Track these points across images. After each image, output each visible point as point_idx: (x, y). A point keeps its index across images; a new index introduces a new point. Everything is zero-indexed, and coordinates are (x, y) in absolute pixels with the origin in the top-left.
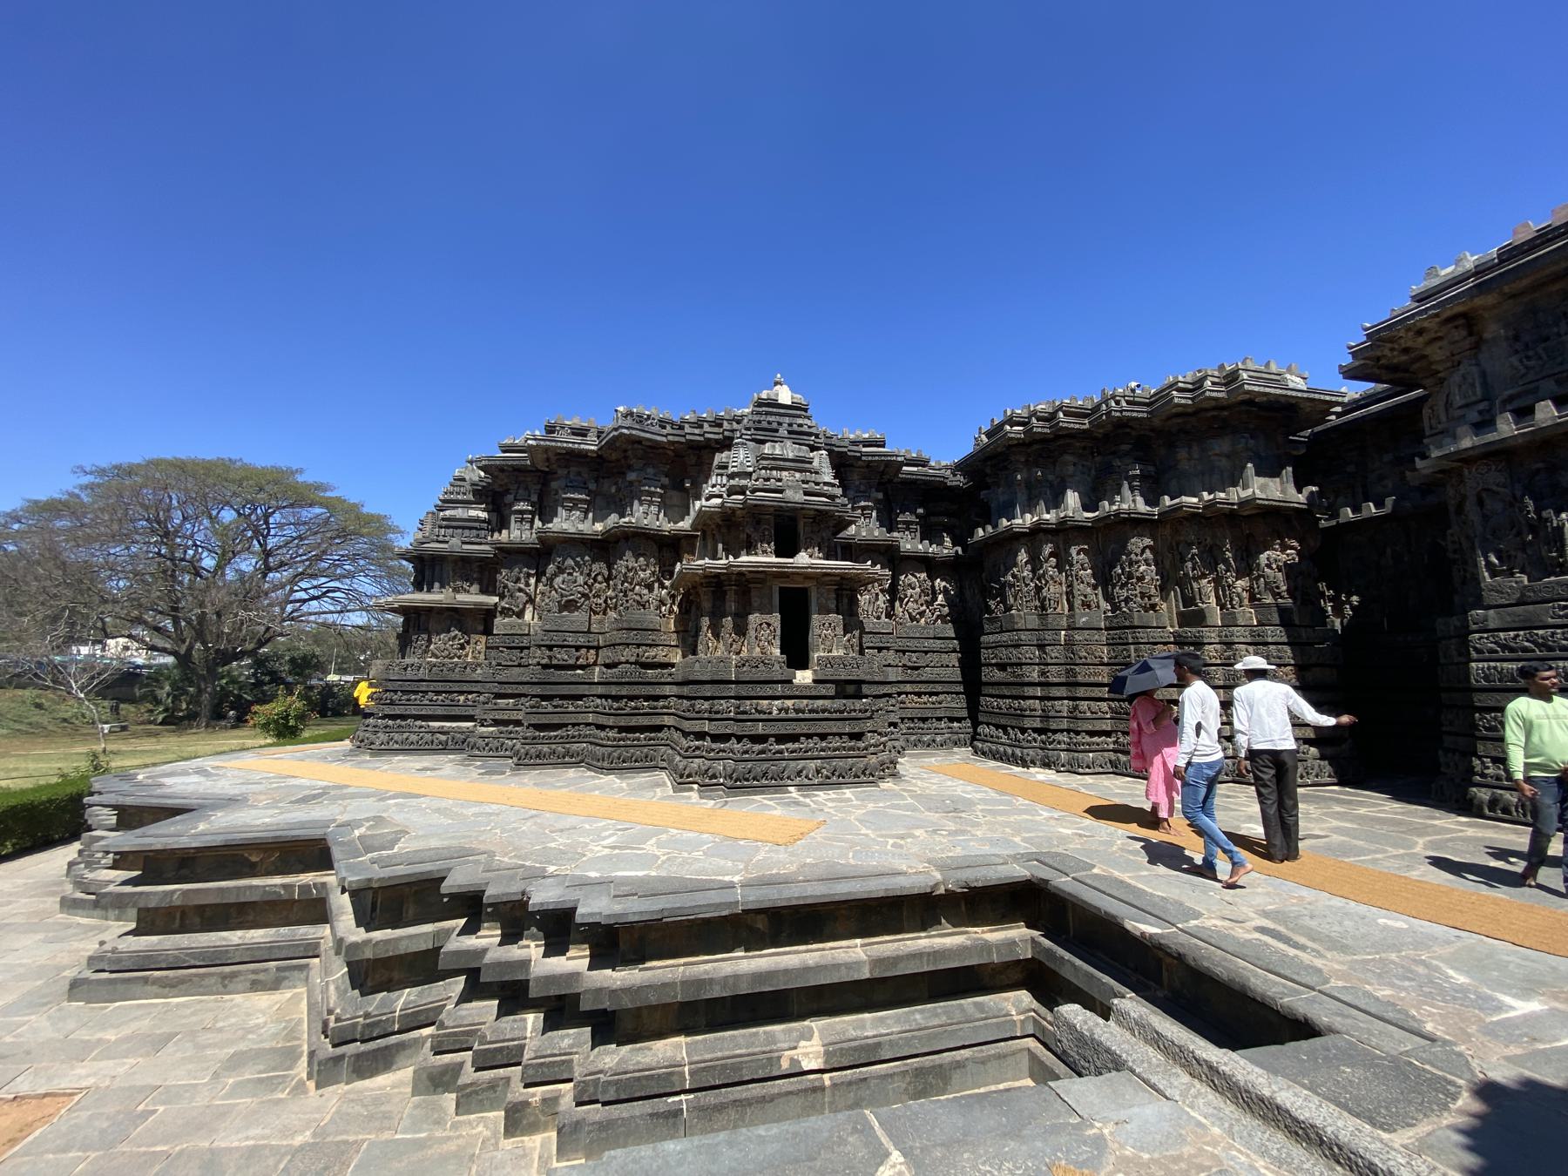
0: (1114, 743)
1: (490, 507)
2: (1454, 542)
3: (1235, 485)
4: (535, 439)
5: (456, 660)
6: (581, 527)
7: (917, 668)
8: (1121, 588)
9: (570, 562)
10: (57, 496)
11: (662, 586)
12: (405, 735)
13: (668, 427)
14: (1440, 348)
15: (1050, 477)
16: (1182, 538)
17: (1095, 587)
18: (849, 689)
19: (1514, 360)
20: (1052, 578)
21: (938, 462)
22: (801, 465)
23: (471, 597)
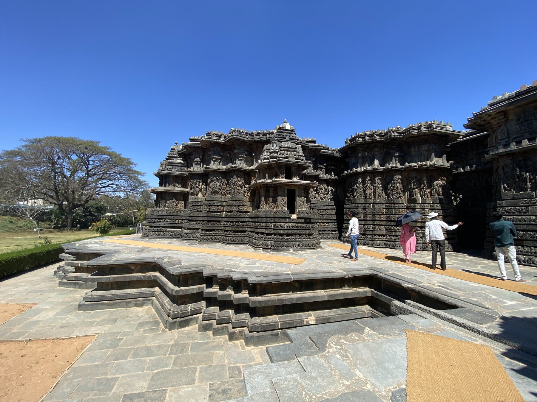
0: (386, 238)
1: (184, 159)
2: (494, 180)
3: (428, 160)
4: (205, 138)
5: (175, 209)
6: (219, 167)
7: (323, 215)
8: (391, 191)
9: (215, 178)
10: (15, 149)
11: (245, 187)
12: (159, 233)
13: (249, 136)
14: (495, 121)
15: (370, 155)
16: (411, 176)
17: (382, 191)
18: (308, 220)
19: (517, 126)
20: (369, 187)
21: (331, 148)
22: (293, 149)
23: (179, 189)
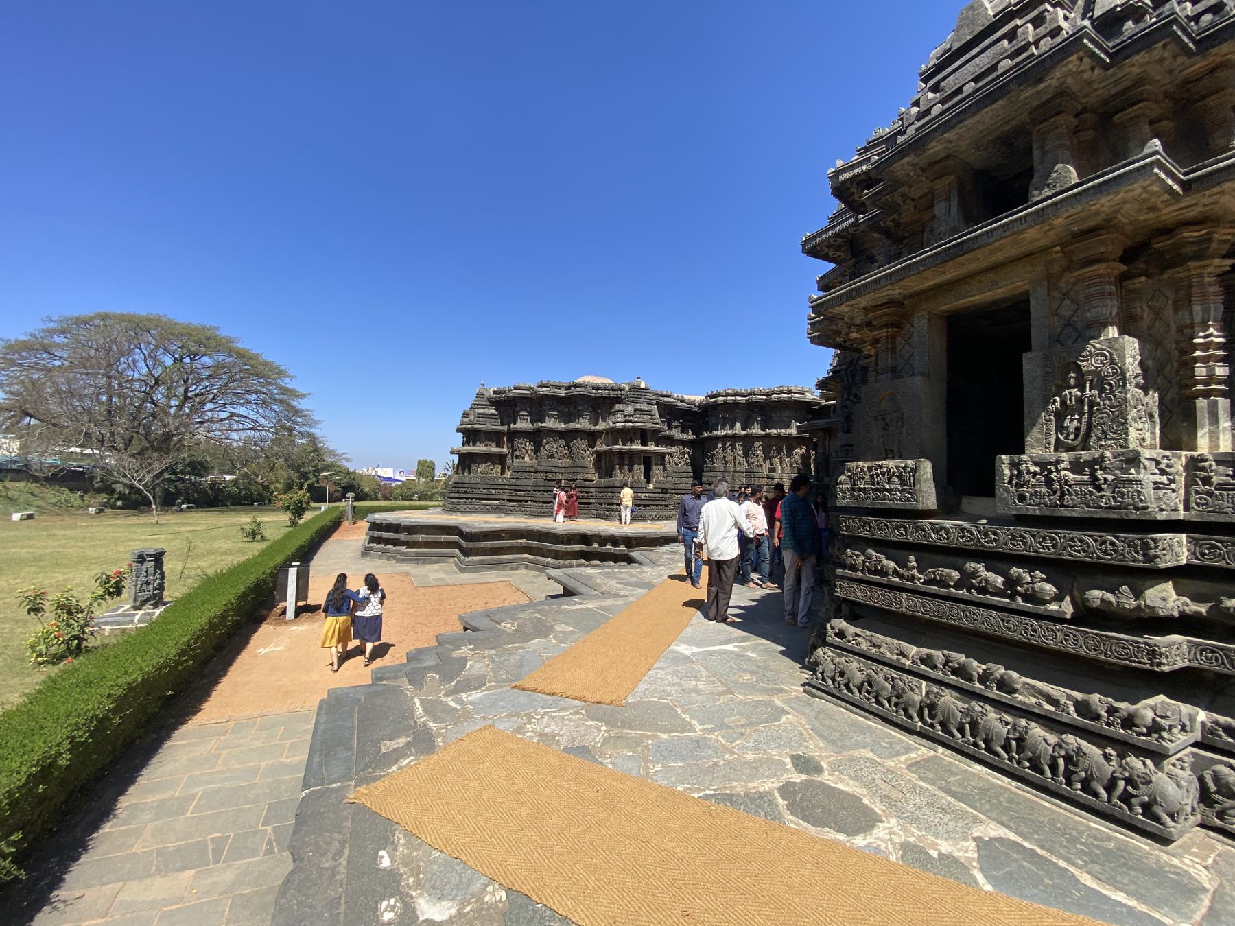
9: (551, 439)
18: (664, 491)
22: (649, 412)
23: (494, 449)
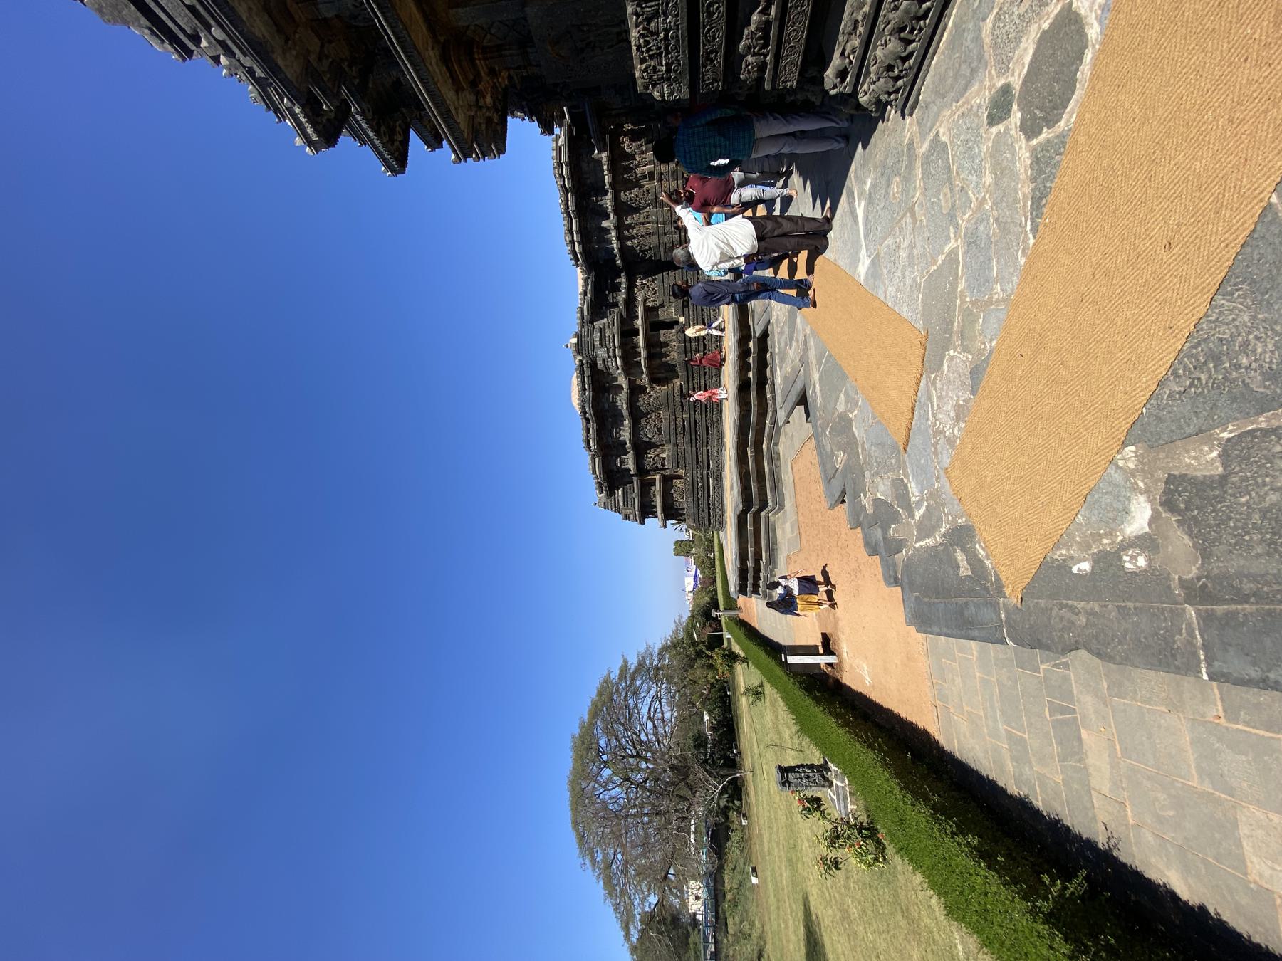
9: (642, 432)
22: (602, 331)
23: (657, 488)
